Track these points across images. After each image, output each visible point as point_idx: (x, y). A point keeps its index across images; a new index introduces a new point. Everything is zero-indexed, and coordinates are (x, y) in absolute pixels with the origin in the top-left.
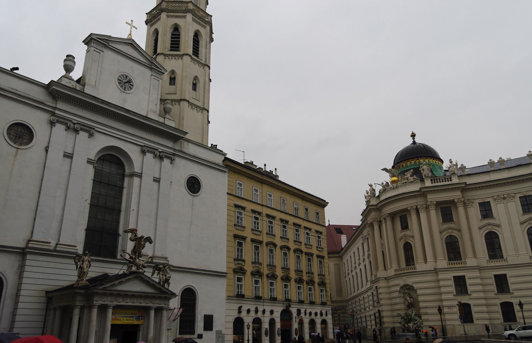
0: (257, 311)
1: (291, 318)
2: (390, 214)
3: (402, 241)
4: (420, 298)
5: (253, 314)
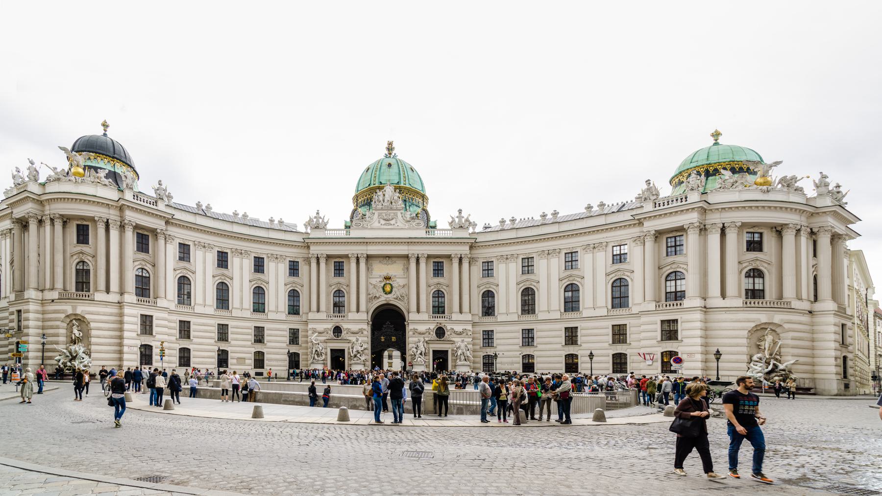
2: (62, 216)
3: (75, 257)
4: (93, 333)
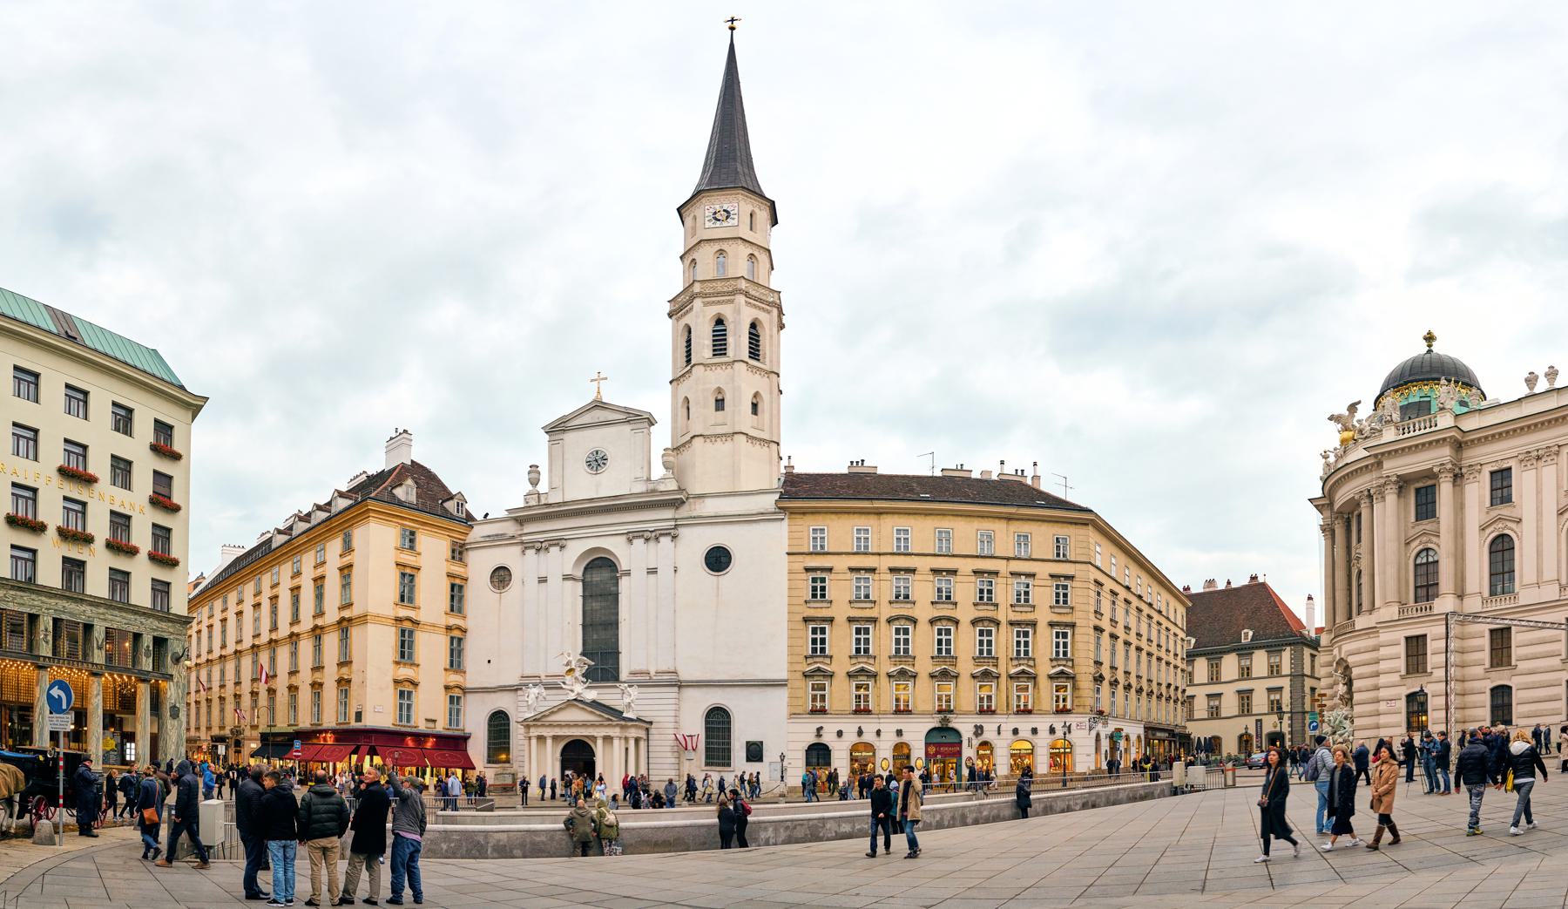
0: (860, 733)
1: (960, 743)
5: (851, 738)
